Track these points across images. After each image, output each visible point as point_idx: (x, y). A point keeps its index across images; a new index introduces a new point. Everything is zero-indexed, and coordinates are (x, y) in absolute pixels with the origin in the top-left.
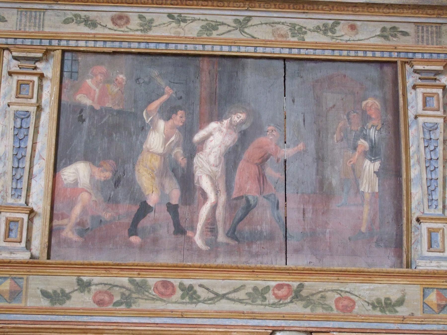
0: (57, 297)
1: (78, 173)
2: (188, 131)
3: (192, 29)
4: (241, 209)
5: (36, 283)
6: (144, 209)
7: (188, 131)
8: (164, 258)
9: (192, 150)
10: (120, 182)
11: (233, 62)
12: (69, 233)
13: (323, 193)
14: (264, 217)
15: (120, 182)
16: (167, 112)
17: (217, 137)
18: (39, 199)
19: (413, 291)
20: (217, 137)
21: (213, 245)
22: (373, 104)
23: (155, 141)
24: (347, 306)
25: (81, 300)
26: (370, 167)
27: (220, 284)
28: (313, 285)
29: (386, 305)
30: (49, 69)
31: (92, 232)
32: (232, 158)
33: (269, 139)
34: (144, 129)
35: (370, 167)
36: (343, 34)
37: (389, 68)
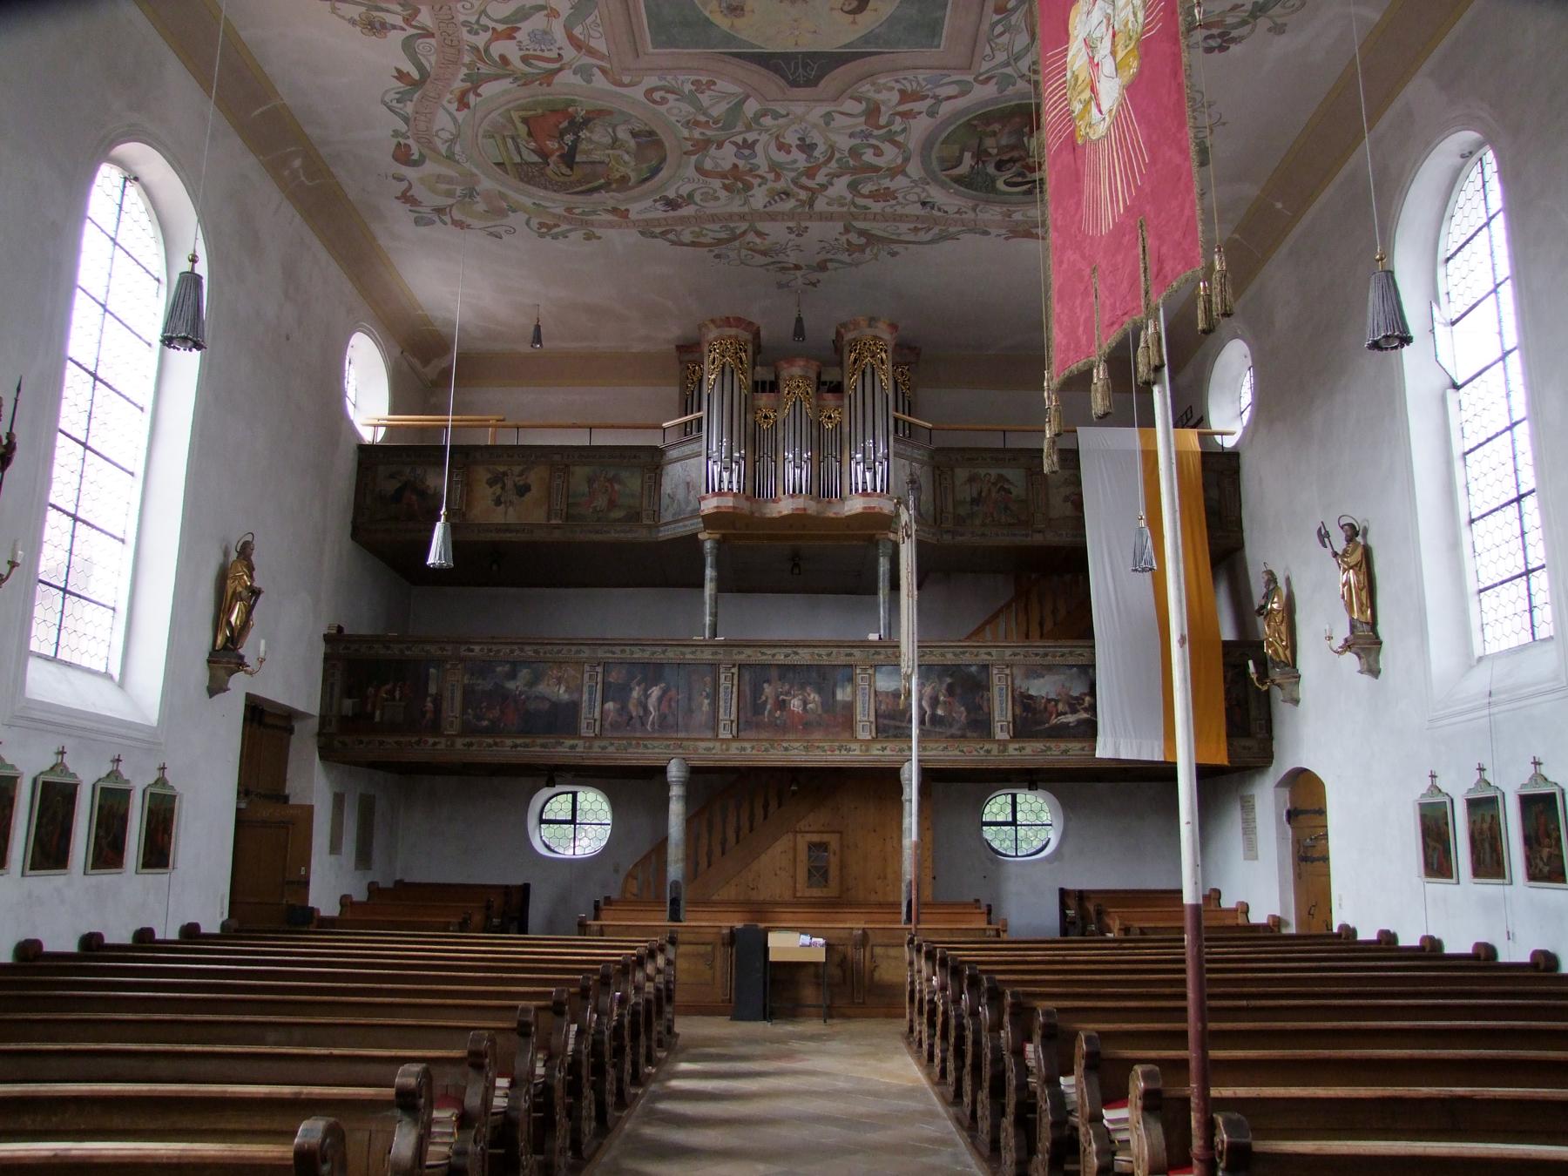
0: (604, 748)
1: (610, 705)
2: (646, 690)
3: (647, 654)
4: (663, 717)
5: (597, 743)
6: (631, 718)
7: (646, 690)
8: (638, 735)
9: (647, 697)
10: (623, 708)
11: (660, 666)
12: (607, 725)
13: (690, 711)
14: (670, 719)
15: (623, 708)
16: (639, 684)
17: (655, 692)
18: (597, 715)
19: (718, 744)
20: (655, 692)
21: (654, 730)
22: (708, 679)
23: (635, 694)
24: (696, 749)
25: (611, 749)
26: (706, 701)
27: (656, 743)
28: (685, 743)
29: (709, 749)
30: (599, 669)
31: (615, 726)
32: (660, 699)
33: (673, 692)
34: (631, 690)
35: (706, 701)
36: (699, 655)
37: (714, 666)
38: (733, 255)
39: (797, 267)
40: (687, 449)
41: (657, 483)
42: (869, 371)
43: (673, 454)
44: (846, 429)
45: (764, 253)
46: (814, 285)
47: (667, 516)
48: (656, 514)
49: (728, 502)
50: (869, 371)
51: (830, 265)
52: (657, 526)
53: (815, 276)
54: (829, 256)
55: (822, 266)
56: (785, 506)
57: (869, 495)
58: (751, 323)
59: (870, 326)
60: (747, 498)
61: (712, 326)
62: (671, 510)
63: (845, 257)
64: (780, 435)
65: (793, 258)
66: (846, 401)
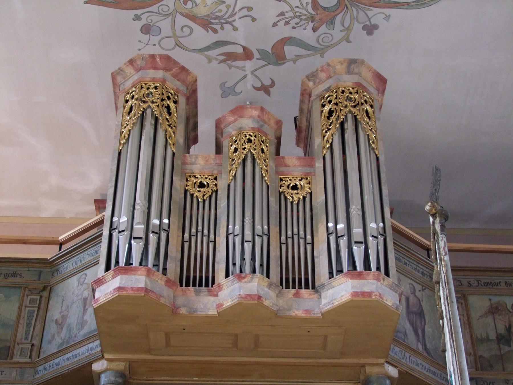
38: (165, 25)
39: (247, 55)
40: (86, 257)
41: (43, 308)
42: (349, 126)
43: (69, 266)
44: (319, 198)
45: (206, 23)
46: (266, 89)
47: (50, 348)
48: (36, 349)
49: (139, 280)
50: (349, 126)
51: (290, 51)
52: (34, 366)
53: (270, 72)
54: (286, 32)
55: (277, 56)
56: (229, 292)
57: (360, 276)
58: (183, 69)
59: (349, 72)
60: (169, 283)
61: (130, 70)
62: (58, 340)
63: (306, 34)
64: (222, 203)
65: (240, 35)
66: (319, 165)
